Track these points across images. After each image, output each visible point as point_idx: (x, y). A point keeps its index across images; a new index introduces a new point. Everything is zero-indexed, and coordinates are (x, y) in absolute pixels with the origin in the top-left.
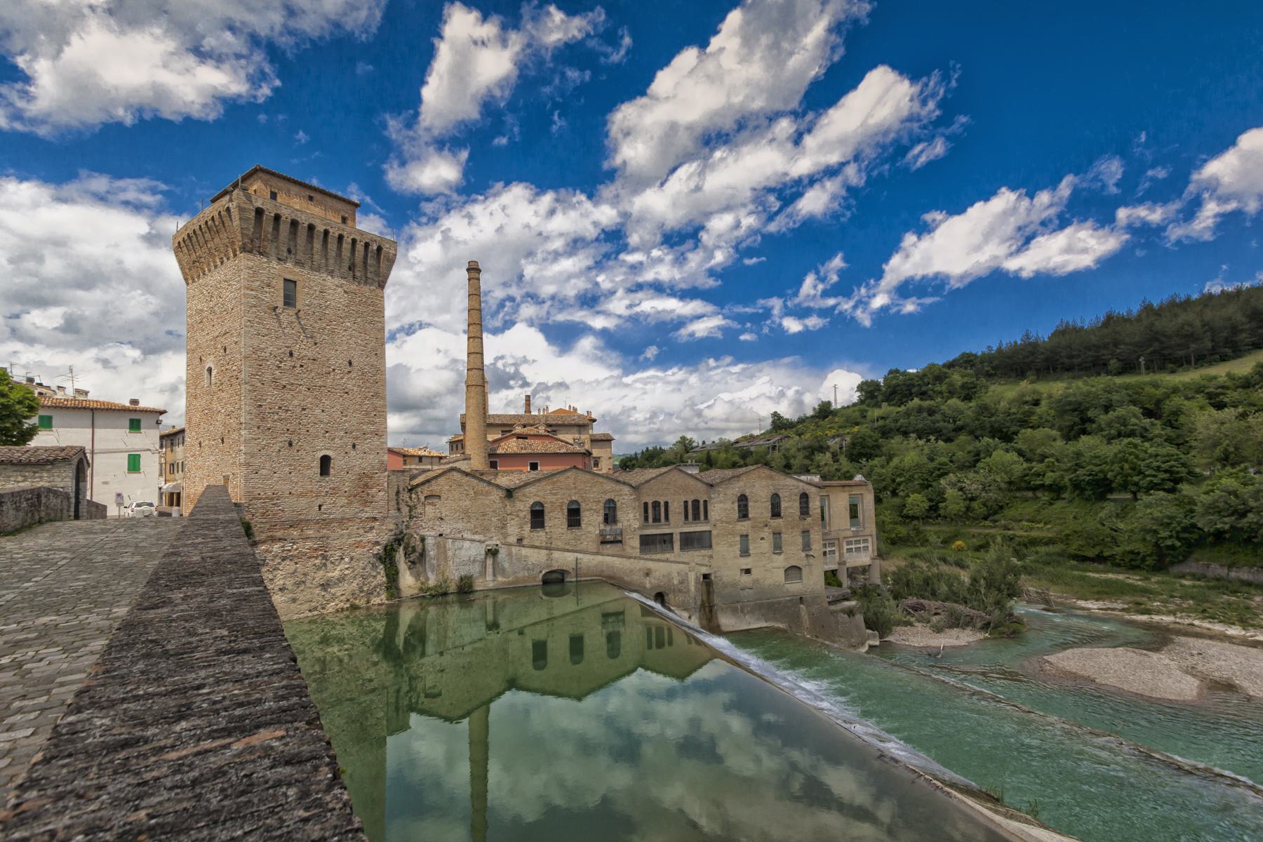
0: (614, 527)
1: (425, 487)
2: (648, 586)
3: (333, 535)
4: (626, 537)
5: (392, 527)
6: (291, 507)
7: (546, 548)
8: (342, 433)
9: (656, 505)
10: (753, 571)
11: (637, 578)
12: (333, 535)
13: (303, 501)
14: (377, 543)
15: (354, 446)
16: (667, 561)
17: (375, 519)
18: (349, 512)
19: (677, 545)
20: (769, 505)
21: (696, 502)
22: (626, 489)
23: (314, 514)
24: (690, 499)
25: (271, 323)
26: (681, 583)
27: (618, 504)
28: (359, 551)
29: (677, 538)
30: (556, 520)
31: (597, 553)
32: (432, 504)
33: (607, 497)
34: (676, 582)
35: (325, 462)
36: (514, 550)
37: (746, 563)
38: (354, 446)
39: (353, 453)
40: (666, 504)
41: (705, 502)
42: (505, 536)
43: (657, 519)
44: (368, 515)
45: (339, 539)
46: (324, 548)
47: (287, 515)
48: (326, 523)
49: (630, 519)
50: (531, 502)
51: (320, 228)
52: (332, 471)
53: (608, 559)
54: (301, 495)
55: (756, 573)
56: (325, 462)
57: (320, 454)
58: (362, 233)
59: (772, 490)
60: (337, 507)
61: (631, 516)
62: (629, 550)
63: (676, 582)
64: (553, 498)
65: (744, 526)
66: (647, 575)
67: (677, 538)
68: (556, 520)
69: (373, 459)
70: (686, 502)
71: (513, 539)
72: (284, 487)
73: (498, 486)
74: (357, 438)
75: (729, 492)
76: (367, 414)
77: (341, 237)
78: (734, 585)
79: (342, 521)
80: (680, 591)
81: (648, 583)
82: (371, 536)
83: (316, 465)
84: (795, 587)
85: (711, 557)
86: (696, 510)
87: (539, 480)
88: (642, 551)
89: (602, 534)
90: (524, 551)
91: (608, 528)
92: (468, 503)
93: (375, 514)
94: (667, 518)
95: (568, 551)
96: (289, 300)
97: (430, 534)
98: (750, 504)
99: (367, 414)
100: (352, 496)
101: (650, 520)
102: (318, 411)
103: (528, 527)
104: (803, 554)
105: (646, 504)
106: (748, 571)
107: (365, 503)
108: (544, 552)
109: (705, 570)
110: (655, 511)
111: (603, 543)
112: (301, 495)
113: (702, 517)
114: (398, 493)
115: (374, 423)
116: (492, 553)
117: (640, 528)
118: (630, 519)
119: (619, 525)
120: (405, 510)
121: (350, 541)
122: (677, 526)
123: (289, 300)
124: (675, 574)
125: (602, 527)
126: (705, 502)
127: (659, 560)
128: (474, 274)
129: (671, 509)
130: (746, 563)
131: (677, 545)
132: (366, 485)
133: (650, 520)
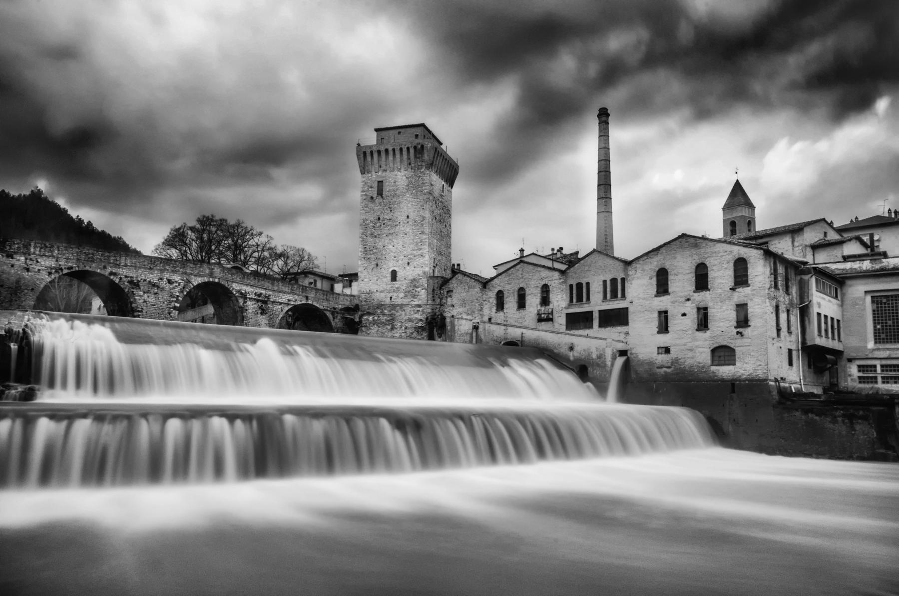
0: (547, 307)
2: (572, 358)
3: (397, 314)
4: (556, 315)
5: (429, 310)
6: (378, 297)
7: (505, 325)
9: (579, 285)
10: (672, 350)
11: (564, 350)
12: (397, 314)
13: (383, 295)
14: (421, 320)
16: (587, 336)
17: (419, 306)
18: (405, 301)
19: (596, 322)
20: (692, 277)
21: (614, 281)
22: (556, 274)
23: (388, 301)
24: (608, 278)
25: (371, 205)
26: (599, 357)
27: (551, 288)
28: (410, 324)
29: (596, 315)
30: (511, 303)
31: (535, 329)
32: (451, 297)
33: (543, 283)
34: (594, 356)
36: (487, 326)
37: (664, 340)
39: (408, 268)
40: (588, 284)
41: (623, 280)
42: (482, 316)
43: (580, 299)
44: (416, 303)
45: (402, 315)
46: (393, 320)
47: (376, 302)
48: (393, 307)
49: (560, 301)
50: (496, 290)
53: (543, 333)
54: (382, 292)
55: (674, 353)
57: (391, 270)
59: (697, 260)
60: (399, 298)
61: (559, 297)
62: (556, 325)
63: (594, 356)
64: (508, 287)
65: (663, 302)
66: (571, 348)
67: (596, 315)
68: (511, 303)
69: (419, 271)
70: (605, 282)
71: (486, 319)
72: (374, 288)
74: (410, 259)
75: (647, 267)
76: (417, 244)
78: (651, 363)
79: (402, 306)
80: (598, 365)
81: (571, 355)
82: (418, 316)
84: (725, 371)
85: (627, 334)
86: (615, 288)
88: (567, 329)
89: (539, 314)
90: (493, 327)
91: (543, 308)
93: (420, 302)
94: (588, 299)
95: (517, 327)
96: (380, 193)
97: (447, 315)
98: (670, 277)
99: (417, 244)
100: (407, 293)
101: (575, 300)
102: (391, 247)
103: (494, 309)
104: (735, 331)
105: (571, 286)
106: (667, 350)
107: (414, 296)
108: (503, 328)
109: (621, 346)
110: (579, 292)
111: (540, 320)
112: (382, 292)
113: (619, 295)
114: (433, 290)
115: (420, 250)
116: (476, 328)
117: (566, 308)
118: (560, 301)
119: (551, 306)
121: (406, 317)
122: (597, 304)
123: (380, 193)
124: (594, 350)
125: (539, 307)
126: (623, 280)
127: (580, 336)
128: (604, 119)
129: (592, 289)
130: (664, 340)
131: (596, 322)
132: (415, 286)
133: (575, 300)
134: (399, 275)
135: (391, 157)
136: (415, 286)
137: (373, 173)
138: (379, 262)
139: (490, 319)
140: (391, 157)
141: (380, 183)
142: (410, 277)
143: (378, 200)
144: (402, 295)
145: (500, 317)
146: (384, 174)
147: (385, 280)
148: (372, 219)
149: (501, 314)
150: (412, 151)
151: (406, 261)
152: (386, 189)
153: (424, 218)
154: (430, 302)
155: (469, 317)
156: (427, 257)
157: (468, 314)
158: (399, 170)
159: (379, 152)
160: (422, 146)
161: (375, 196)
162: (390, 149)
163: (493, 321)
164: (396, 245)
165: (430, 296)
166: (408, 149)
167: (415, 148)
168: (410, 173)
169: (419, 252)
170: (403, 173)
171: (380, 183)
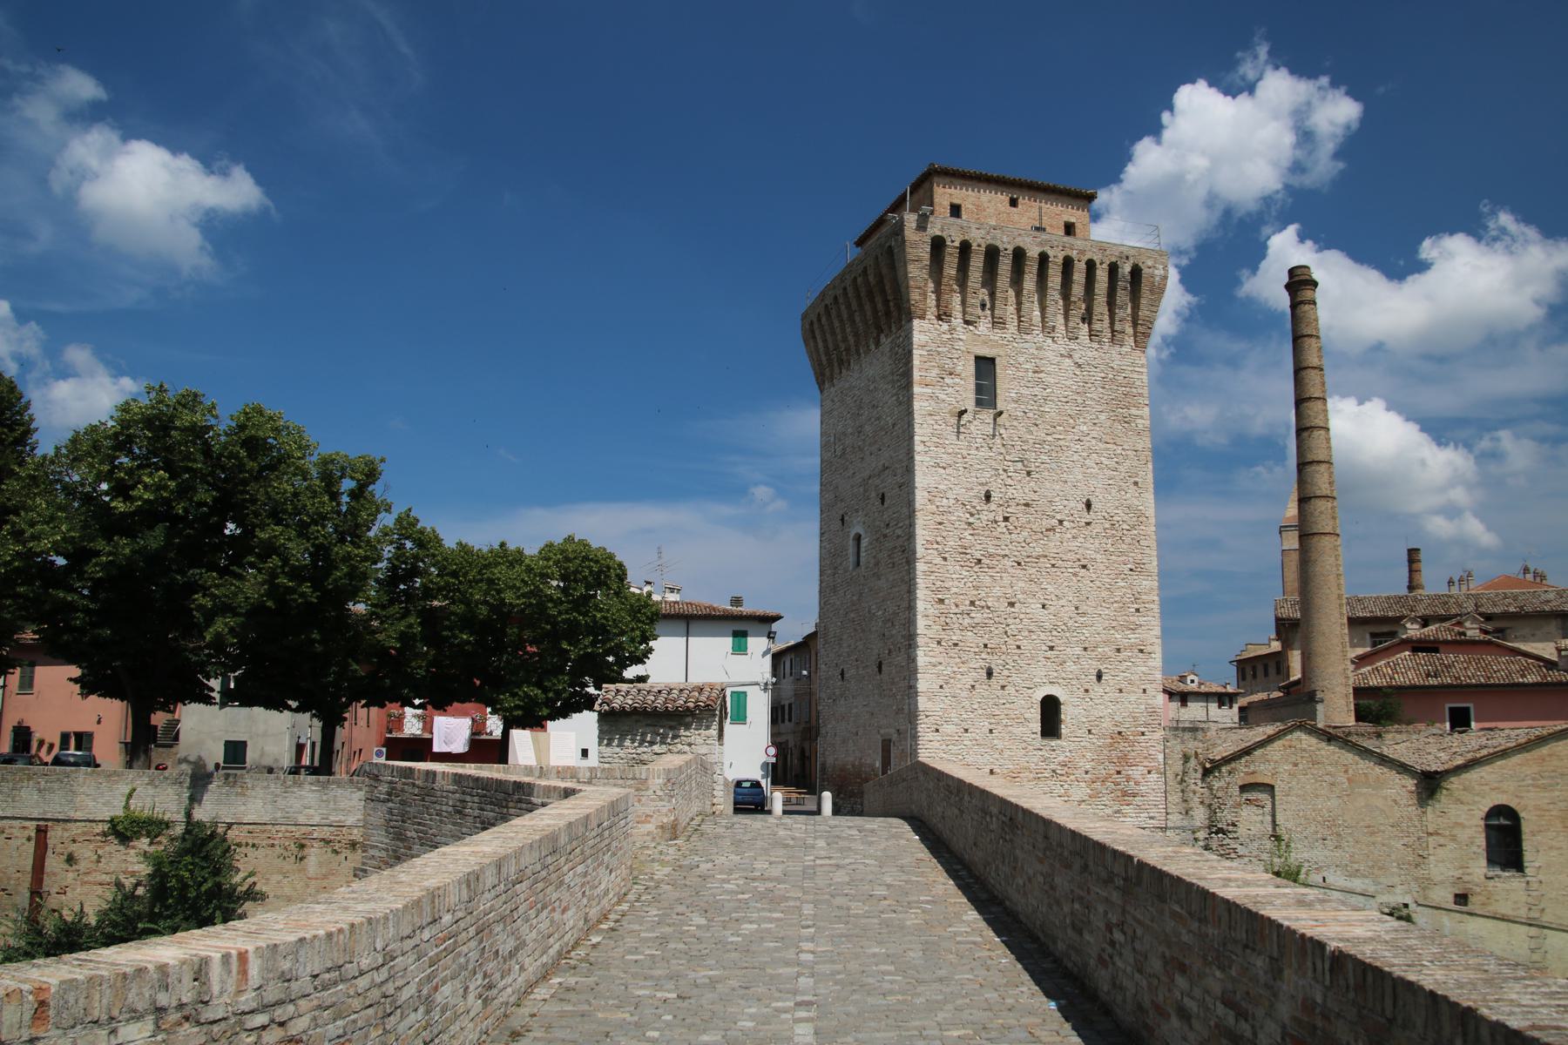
1: (1241, 765)
8: (1078, 651)
15: (1099, 676)
35: (1050, 711)
36: (1447, 921)
38: (1099, 676)
39: (1098, 690)
51: (1033, 252)
52: (1064, 730)
56: (1050, 711)
58: (1102, 247)
69: (1133, 703)
71: (1444, 896)
73: (1403, 768)
74: (1103, 659)
77: (1068, 264)
83: (1035, 714)
87: (1504, 754)
92: (1333, 803)
120: (1200, 815)
132: (1124, 759)
134: (1070, 714)
135: (1029, 283)
136: (1124, 759)
137: (957, 321)
138: (996, 663)
139: (1462, 899)
140: (1029, 283)
141: (985, 366)
142: (1107, 724)
143: (980, 423)
144: (1080, 791)
145: (1508, 890)
146: (996, 335)
147: (1018, 730)
148: (964, 497)
149: (1509, 883)
150: (1102, 275)
151: (1096, 665)
152: (1007, 387)
153: (1140, 515)
154: (1175, 819)
155: (1357, 884)
156: (1158, 656)
157: (1355, 874)
158: (1048, 330)
159: (992, 254)
160: (1136, 272)
161: (970, 404)
162: (1033, 252)
163: (1475, 904)
164: (1054, 606)
165: (1175, 798)
166: (1091, 265)
167: (1113, 269)
168: (1085, 349)
169: (1133, 638)
170: (1062, 345)
171: (985, 366)
